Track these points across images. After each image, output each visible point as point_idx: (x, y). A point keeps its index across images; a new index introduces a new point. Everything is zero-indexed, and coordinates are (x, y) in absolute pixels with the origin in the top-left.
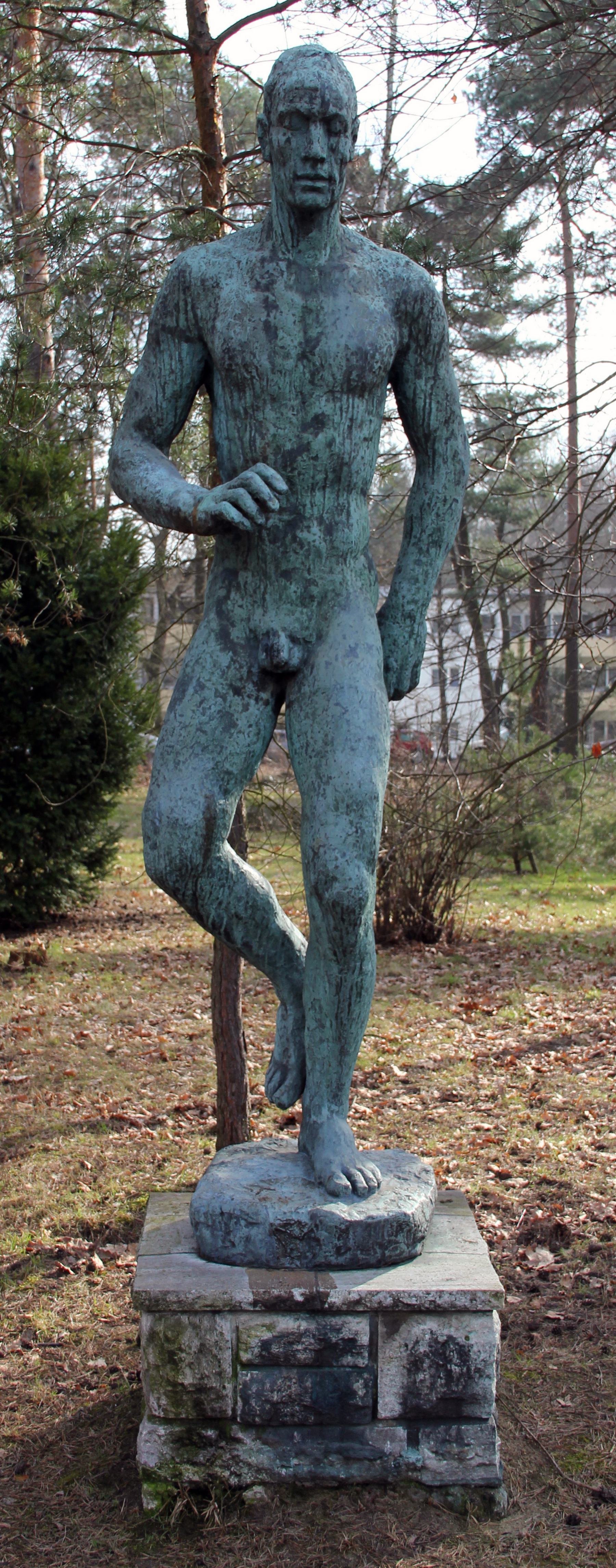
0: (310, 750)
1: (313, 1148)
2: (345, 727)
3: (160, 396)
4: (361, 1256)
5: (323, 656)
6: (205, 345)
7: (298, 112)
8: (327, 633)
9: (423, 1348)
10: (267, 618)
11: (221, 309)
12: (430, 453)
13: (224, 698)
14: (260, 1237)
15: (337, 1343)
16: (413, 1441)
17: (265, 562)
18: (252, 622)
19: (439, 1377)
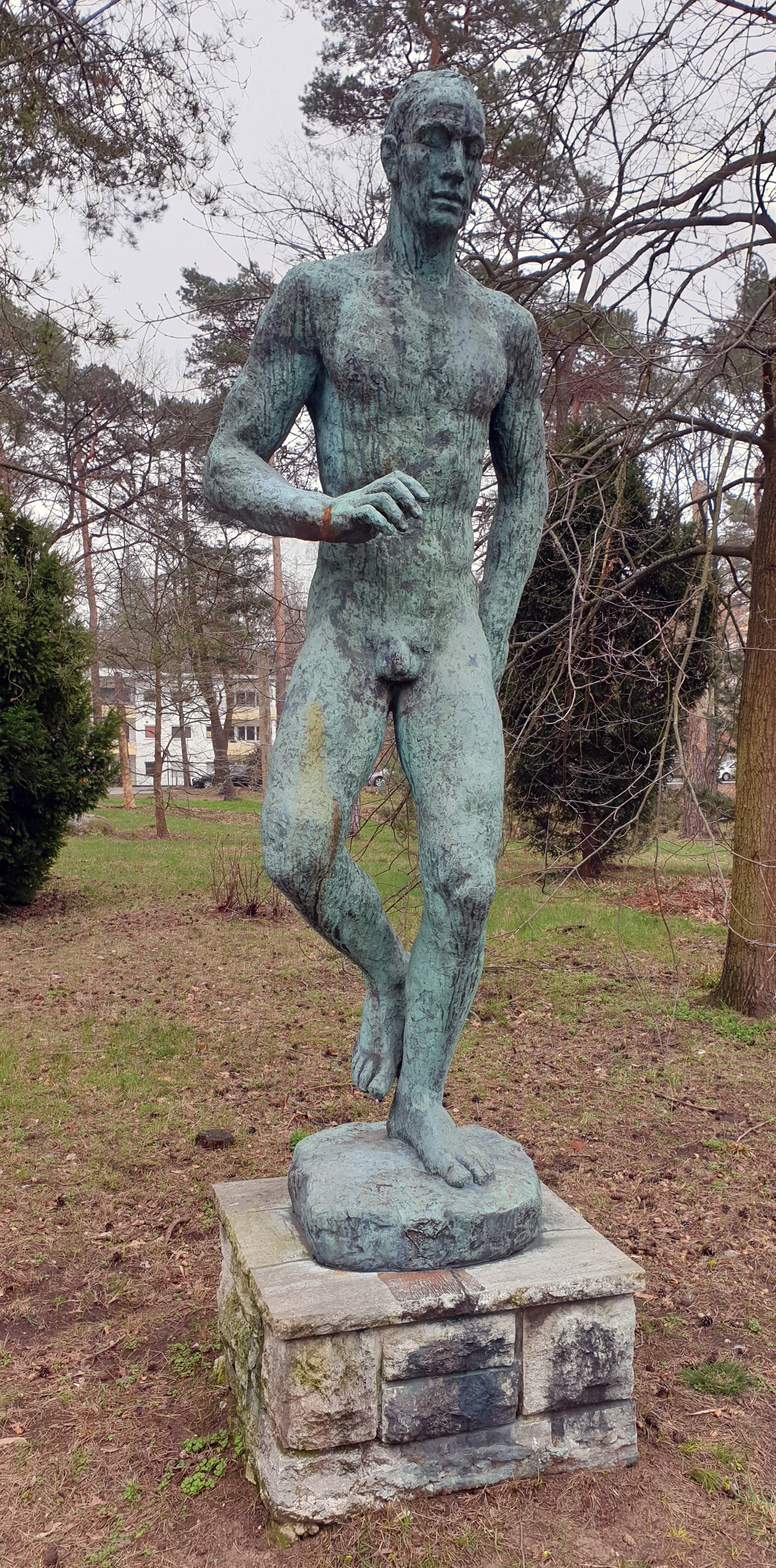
0: (433, 754)
1: (419, 1137)
2: (474, 732)
3: (269, 406)
4: (492, 1248)
5: (442, 663)
6: (319, 358)
7: (442, 126)
8: (446, 643)
9: (570, 1339)
10: (386, 628)
11: (343, 321)
12: (519, 485)
13: (345, 702)
14: (391, 1239)
15: (486, 1346)
16: (558, 1432)
17: (385, 574)
18: (369, 631)
19: (586, 1366)
